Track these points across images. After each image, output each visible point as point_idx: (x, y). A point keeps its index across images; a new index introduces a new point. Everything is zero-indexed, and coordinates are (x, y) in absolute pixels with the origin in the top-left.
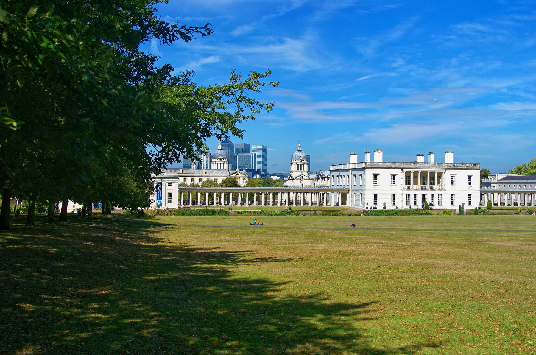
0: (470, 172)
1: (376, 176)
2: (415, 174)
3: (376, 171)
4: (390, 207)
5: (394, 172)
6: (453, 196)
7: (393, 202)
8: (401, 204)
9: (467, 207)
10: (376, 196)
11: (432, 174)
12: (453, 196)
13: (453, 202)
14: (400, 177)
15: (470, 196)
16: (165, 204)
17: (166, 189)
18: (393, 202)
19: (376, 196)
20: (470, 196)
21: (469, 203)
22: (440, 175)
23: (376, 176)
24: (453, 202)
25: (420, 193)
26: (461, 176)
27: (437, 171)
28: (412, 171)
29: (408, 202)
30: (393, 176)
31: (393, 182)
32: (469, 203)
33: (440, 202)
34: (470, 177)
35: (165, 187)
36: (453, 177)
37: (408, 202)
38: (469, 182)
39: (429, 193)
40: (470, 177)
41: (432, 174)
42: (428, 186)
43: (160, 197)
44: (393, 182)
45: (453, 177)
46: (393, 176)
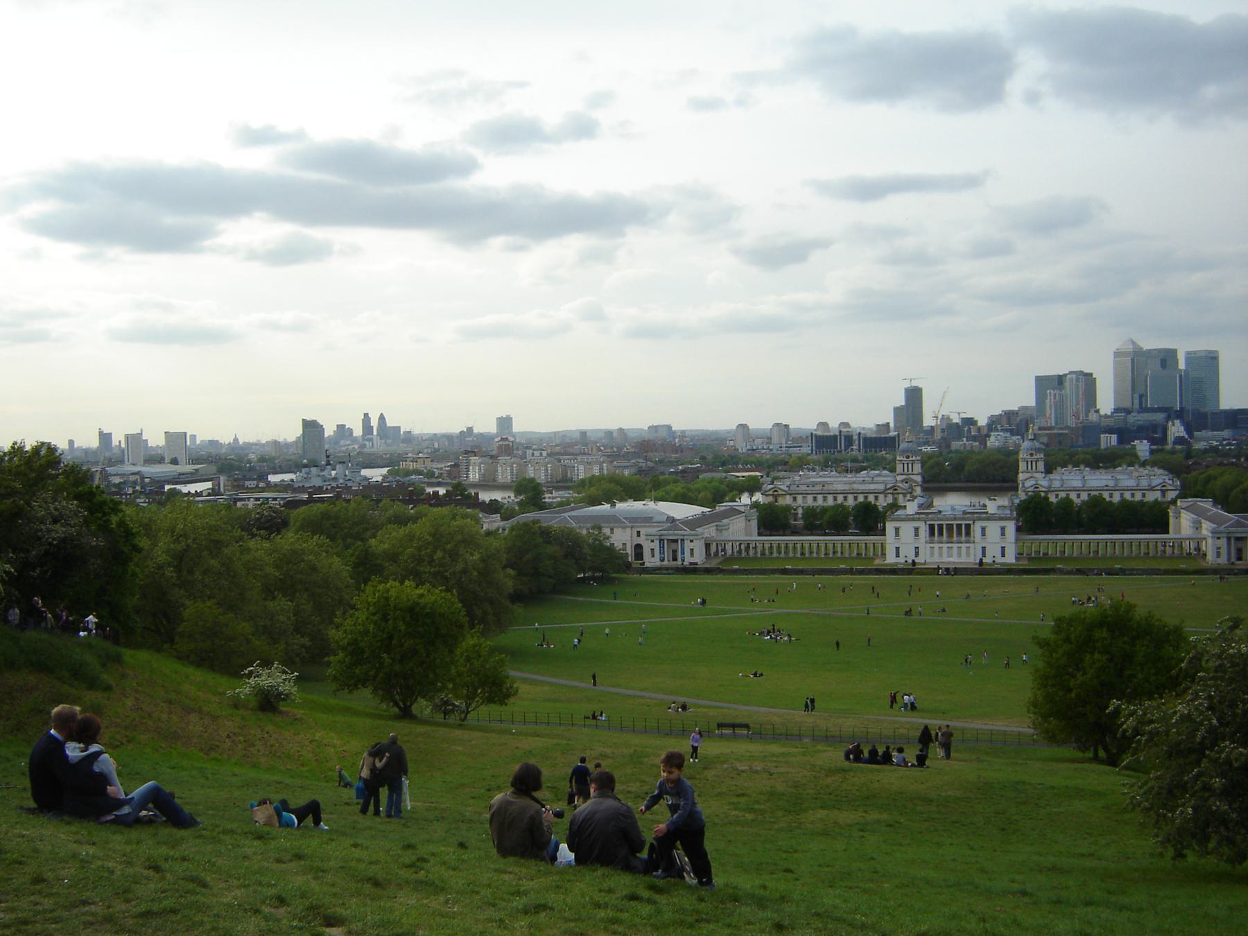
0: (1003, 523)
1: (897, 530)
2: (940, 527)
3: (897, 524)
5: (916, 524)
6: (984, 548)
7: (917, 554)
9: (1000, 560)
10: (898, 549)
12: (984, 548)
15: (1003, 548)
16: (688, 560)
17: (688, 545)
18: (917, 554)
19: (898, 549)
20: (1003, 548)
21: (1003, 555)
22: (968, 526)
23: (897, 530)
26: (993, 528)
27: (963, 522)
28: (936, 523)
29: (932, 554)
30: (917, 529)
31: (917, 534)
32: (1003, 555)
33: (968, 554)
34: (1003, 529)
35: (687, 543)
36: (983, 529)
37: (932, 554)
38: (1003, 534)
40: (1003, 529)
41: (959, 526)
42: (955, 538)
43: (683, 553)
44: (917, 534)
45: (983, 529)
46: (917, 529)
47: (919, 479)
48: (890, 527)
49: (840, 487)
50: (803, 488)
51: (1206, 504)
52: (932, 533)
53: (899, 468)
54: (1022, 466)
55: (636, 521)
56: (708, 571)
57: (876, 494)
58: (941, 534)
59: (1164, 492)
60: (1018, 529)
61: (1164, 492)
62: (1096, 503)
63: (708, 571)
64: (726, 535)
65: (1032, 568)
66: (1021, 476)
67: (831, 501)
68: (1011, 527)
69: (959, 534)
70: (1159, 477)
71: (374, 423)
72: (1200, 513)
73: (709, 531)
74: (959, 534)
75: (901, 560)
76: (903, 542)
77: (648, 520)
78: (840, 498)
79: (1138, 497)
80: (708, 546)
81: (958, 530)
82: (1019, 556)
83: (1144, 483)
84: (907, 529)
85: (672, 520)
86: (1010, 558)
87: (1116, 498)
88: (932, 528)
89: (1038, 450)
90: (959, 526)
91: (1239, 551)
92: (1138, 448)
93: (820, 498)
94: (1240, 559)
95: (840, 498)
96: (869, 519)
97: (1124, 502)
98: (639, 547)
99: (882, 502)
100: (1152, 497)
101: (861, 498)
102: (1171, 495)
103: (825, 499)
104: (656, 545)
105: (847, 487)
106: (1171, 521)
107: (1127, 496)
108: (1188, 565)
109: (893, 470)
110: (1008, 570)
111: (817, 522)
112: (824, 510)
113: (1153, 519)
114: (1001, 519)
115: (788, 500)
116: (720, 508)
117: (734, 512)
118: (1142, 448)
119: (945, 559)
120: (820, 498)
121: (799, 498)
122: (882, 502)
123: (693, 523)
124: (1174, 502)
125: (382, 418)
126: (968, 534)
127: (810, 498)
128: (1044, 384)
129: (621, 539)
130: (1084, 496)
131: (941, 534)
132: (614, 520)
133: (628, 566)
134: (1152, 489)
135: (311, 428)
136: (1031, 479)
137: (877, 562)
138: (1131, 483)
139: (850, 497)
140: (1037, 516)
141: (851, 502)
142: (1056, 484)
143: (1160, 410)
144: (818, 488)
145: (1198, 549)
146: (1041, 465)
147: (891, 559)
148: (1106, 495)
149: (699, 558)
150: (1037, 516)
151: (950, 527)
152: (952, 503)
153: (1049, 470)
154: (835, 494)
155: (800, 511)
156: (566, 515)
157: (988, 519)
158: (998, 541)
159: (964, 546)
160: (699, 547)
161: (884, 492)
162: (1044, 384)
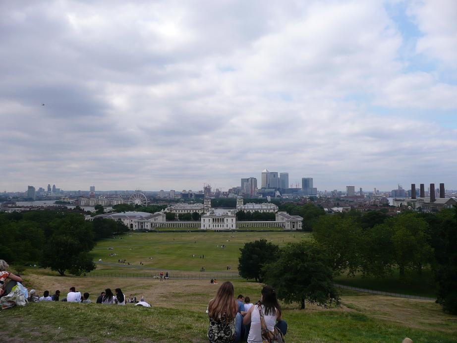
1: (204, 220)
4: (208, 228)
5: (209, 218)
7: (209, 227)
8: (211, 228)
11: (221, 219)
13: (227, 227)
14: (211, 219)
16: (146, 228)
18: (209, 227)
22: (223, 219)
23: (204, 220)
24: (227, 227)
25: (217, 224)
26: (230, 219)
39: (220, 224)
47: (210, 206)
48: (202, 219)
49: (189, 208)
50: (179, 208)
51: (285, 213)
52: (213, 221)
53: (205, 203)
54: (238, 203)
55: (131, 217)
56: (151, 231)
57: (199, 210)
58: (216, 221)
59: (274, 210)
60: (236, 220)
61: (274, 210)
62: (256, 212)
63: (151, 231)
64: (156, 222)
65: (240, 230)
66: (237, 206)
67: (186, 212)
68: (234, 219)
69: (221, 221)
70: (273, 206)
71: (52, 188)
72: (283, 215)
73: (152, 220)
74: (221, 221)
75: (205, 228)
76: (206, 223)
77: (134, 217)
78: (189, 211)
79: (268, 211)
80: (152, 224)
81: (220, 220)
82: (237, 226)
83: (269, 208)
84: (207, 219)
85: (141, 217)
86: (234, 228)
87: (262, 212)
88: (213, 219)
89: (242, 199)
90: (221, 219)
91: (294, 226)
92: (268, 198)
93: (183, 211)
94: (294, 227)
95: (189, 211)
96: (197, 217)
97: (264, 212)
98: (132, 224)
99: (200, 212)
100: (271, 211)
101: (194, 211)
102: (276, 211)
103: (185, 211)
104: (137, 223)
105: (191, 208)
106: (276, 218)
107: (265, 211)
108: (281, 229)
109: (203, 203)
110: (234, 231)
111: (184, 217)
112: (184, 214)
113: (271, 217)
114: (233, 217)
115: (174, 212)
116: (155, 214)
117: (159, 215)
118: (269, 198)
119: (217, 228)
120: (183, 211)
121: (178, 211)
122: (200, 212)
123: (148, 218)
124: (277, 213)
125: (54, 186)
126: (223, 221)
127: (180, 211)
128: (243, 181)
129: (126, 222)
130: (254, 211)
131: (216, 221)
132: (125, 217)
133: (129, 230)
134: (271, 209)
135: (31, 188)
136: (240, 206)
137: (199, 229)
138: (266, 207)
139: (192, 211)
140: (241, 216)
141: (192, 212)
142: (246, 208)
143: (274, 188)
144: (183, 208)
145: (283, 225)
146: (242, 203)
147: (202, 228)
148: (259, 211)
149: (149, 228)
150: (241, 216)
151: (218, 219)
152: (219, 212)
153: (244, 204)
154: (187, 210)
155: (178, 215)
156: (110, 215)
157: (229, 217)
158: (231, 223)
159: (222, 224)
160: (149, 224)
161: (201, 210)
162: (243, 181)
